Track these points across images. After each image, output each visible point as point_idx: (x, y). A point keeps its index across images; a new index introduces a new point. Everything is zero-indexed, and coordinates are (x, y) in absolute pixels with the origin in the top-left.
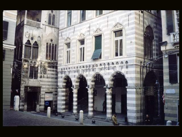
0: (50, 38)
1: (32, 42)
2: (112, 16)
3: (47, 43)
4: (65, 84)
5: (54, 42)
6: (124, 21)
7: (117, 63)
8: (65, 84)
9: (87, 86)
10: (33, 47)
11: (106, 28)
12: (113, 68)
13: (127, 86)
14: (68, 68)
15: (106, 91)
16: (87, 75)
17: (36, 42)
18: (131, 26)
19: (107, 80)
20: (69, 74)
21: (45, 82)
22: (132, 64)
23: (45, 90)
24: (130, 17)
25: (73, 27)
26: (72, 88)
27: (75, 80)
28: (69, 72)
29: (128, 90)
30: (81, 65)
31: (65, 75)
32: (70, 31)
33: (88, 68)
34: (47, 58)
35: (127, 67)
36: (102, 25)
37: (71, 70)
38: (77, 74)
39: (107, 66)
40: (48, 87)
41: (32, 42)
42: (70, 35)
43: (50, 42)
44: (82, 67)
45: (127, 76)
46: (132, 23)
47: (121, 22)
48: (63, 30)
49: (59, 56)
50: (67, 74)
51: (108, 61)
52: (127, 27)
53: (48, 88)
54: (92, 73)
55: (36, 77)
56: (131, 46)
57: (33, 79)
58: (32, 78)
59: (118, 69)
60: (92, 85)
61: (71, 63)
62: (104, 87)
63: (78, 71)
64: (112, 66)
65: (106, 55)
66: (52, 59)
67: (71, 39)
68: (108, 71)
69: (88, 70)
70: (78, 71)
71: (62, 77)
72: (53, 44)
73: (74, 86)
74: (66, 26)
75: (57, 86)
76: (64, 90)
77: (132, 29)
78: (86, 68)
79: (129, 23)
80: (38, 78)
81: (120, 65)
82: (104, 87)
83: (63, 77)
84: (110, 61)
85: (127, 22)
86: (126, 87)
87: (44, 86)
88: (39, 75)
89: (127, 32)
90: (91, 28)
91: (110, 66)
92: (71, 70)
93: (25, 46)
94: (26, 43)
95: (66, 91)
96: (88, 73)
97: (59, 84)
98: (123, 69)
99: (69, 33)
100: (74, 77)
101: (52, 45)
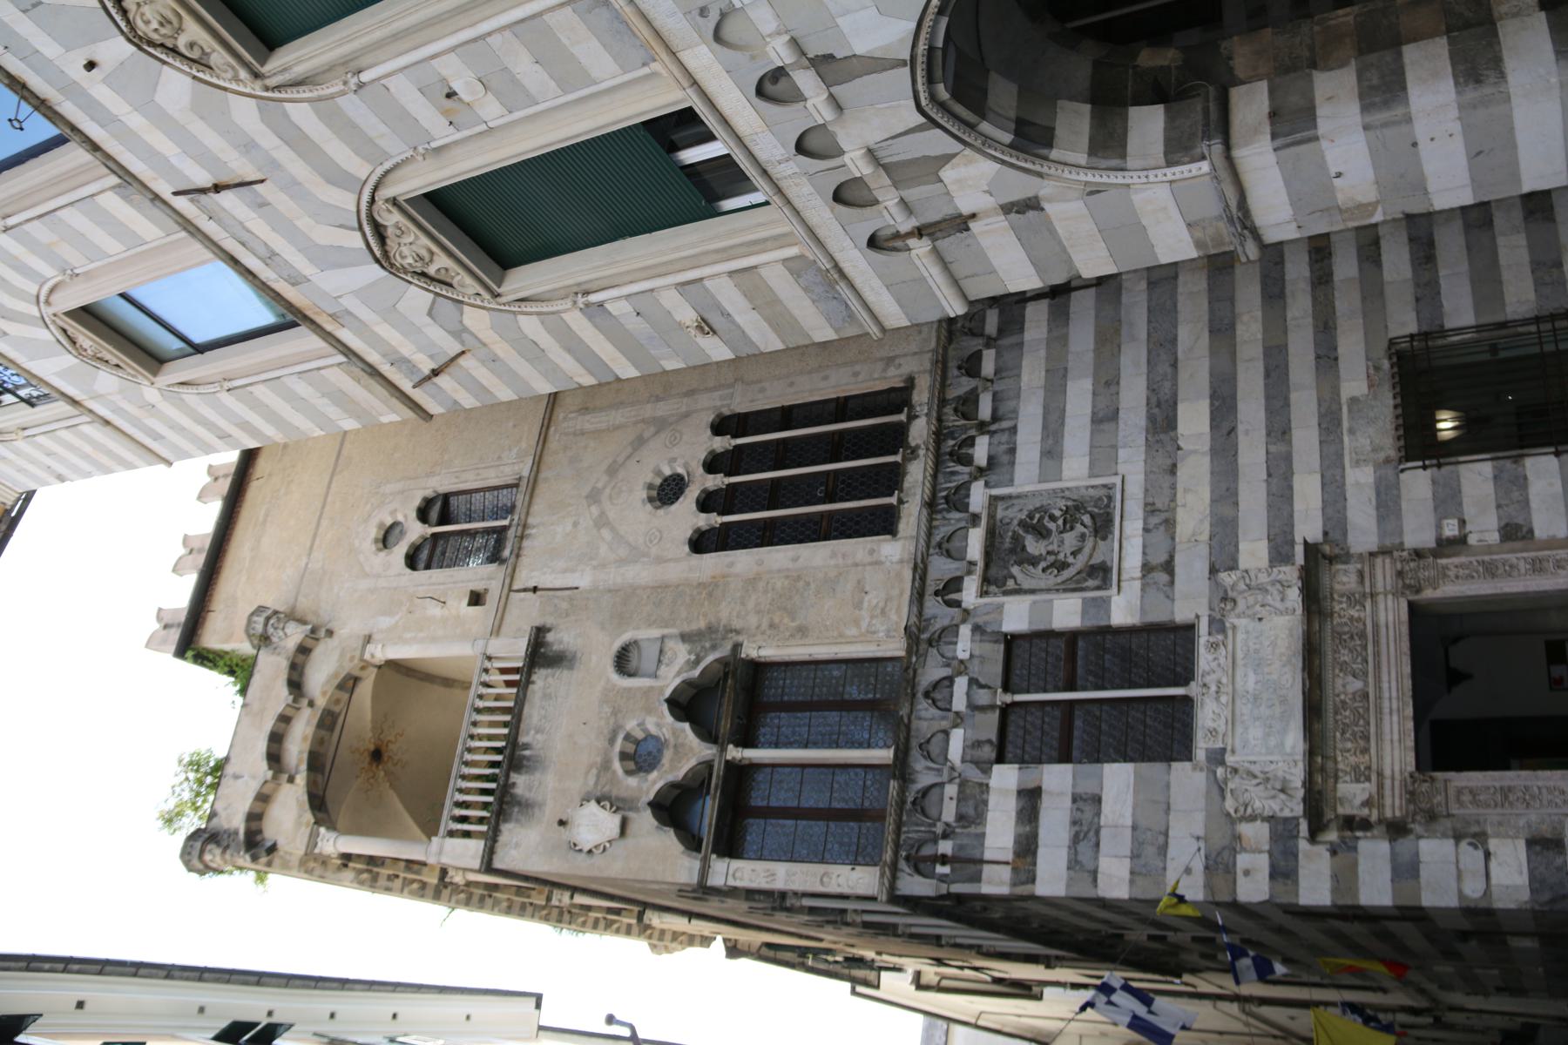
1: (687, 751)
3: (701, 543)
5: (688, 450)
8: (1147, 125)
14: (793, 121)
17: (689, 704)
20: (875, 65)
31: (937, 142)
34: (884, 523)
40: (1306, 439)
41: (687, 751)
43: (686, 517)
49: (716, 350)
55: (1164, 650)
57: (1193, 690)
71: (1031, 205)
83: (1020, 186)
88: (1123, 609)
92: (779, 53)
93: (730, 846)
94: (692, 843)
95: (1292, 71)
97: (1173, 242)
101: (717, 481)
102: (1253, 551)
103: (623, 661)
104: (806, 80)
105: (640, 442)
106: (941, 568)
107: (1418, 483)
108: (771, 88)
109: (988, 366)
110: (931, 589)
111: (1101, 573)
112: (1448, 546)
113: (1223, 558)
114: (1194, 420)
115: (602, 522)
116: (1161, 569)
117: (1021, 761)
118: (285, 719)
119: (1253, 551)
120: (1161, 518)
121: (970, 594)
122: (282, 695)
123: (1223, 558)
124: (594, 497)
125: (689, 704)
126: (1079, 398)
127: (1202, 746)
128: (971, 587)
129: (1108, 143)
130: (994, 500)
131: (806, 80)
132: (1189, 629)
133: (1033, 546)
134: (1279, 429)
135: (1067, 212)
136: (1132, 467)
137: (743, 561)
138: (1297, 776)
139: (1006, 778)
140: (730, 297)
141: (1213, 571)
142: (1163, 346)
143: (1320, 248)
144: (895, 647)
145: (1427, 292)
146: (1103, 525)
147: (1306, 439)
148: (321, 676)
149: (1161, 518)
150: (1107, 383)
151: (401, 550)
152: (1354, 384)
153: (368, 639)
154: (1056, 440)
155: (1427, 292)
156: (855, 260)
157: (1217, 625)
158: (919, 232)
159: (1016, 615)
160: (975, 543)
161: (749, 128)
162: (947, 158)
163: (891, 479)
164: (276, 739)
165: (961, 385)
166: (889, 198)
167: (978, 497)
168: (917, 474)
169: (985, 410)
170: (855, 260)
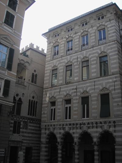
0: (32, 96)
1: (17, 99)
2: (99, 81)
3: (30, 100)
4: (48, 140)
5: (35, 100)
6: (110, 86)
7: (105, 123)
8: (48, 140)
9: (74, 143)
10: (17, 103)
11: (93, 91)
12: (101, 127)
13: (115, 143)
14: (53, 125)
15: (94, 148)
16: (74, 133)
17: (20, 99)
18: (116, 91)
19: (95, 138)
20: (54, 131)
21: (26, 137)
22: (119, 123)
23: (26, 144)
24: (116, 83)
25: (58, 87)
26: (57, 144)
27: (60, 137)
28: (54, 129)
29: (116, 147)
30: (68, 123)
32: (55, 91)
33: (74, 126)
34: (28, 114)
35: (115, 126)
36: (89, 88)
37: (56, 127)
38: (62, 131)
39: (94, 125)
40: (28, 142)
41: (17, 99)
42: (56, 94)
43: (31, 99)
44: (68, 125)
45: (115, 134)
46: (118, 89)
47: (107, 87)
48: (48, 89)
49: (43, 112)
50: (52, 130)
51: (96, 121)
52: (113, 92)
53: (28, 143)
54: (79, 131)
55: (19, 132)
56: (118, 108)
58: (15, 133)
59: (106, 127)
60: (79, 142)
61: (56, 120)
62: (92, 144)
63: (64, 129)
64: (100, 125)
65: (93, 115)
66: (33, 115)
67: (57, 98)
68: (95, 130)
69: (75, 128)
70: (64, 129)
71: (45, 134)
72: (34, 101)
73: (59, 142)
74: (51, 87)
75: (40, 141)
76: (47, 145)
77: (118, 93)
78: (72, 126)
79: (115, 88)
80: (20, 133)
81: (108, 124)
82: (92, 144)
84: (98, 121)
85: (113, 88)
86: (115, 144)
87: (25, 141)
89: (114, 96)
90: (78, 90)
91: (98, 125)
96: (75, 131)
98: (111, 128)
99: (55, 93)
100: (60, 134)
102: (23, 138)
103: (23, 94)
104: (54, 127)
105: (37, 95)
106: (25, 118)
107: (25, 148)
108: (54, 125)
109: (36, 122)
110: (24, 118)
111: (23, 129)
112: (21, 149)
113: (23, 136)
114: (30, 135)
115: (32, 92)
116: (23, 132)
117: (14, 123)
118: (24, 61)
119: (23, 138)
120: (25, 132)
121: (24, 120)
122: (25, 61)
123: (23, 136)
124: (34, 91)
125: (20, 99)
126: (33, 128)
127: (13, 134)
128: (24, 120)
129: (47, 138)
130: (28, 122)
131: (54, 127)
132: (19, 133)
133: (25, 124)
134: (29, 140)
135: (45, 136)
136: (29, 131)
137: (28, 104)
138: (11, 140)
139: (13, 122)
140: (45, 115)
141: (22, 135)
142: (36, 134)
143: (40, 147)
144: (21, 115)
145: (35, 150)
146: (26, 129)
147: (28, 142)
148: (27, 64)
149: (25, 132)
150: (33, 130)
151: (34, 72)
152: (30, 145)
153: (28, 69)
154: (31, 126)
155: (35, 150)
156: (45, 124)
157: (19, 135)
158: (46, 128)
159: (22, 123)
160: (26, 120)
161: (53, 122)
162: (49, 131)
163: (31, 115)
164: (23, 60)
165: (35, 120)
166: (48, 127)
167: (29, 121)
168: (31, 117)
169: (34, 122)
170: (45, 124)
